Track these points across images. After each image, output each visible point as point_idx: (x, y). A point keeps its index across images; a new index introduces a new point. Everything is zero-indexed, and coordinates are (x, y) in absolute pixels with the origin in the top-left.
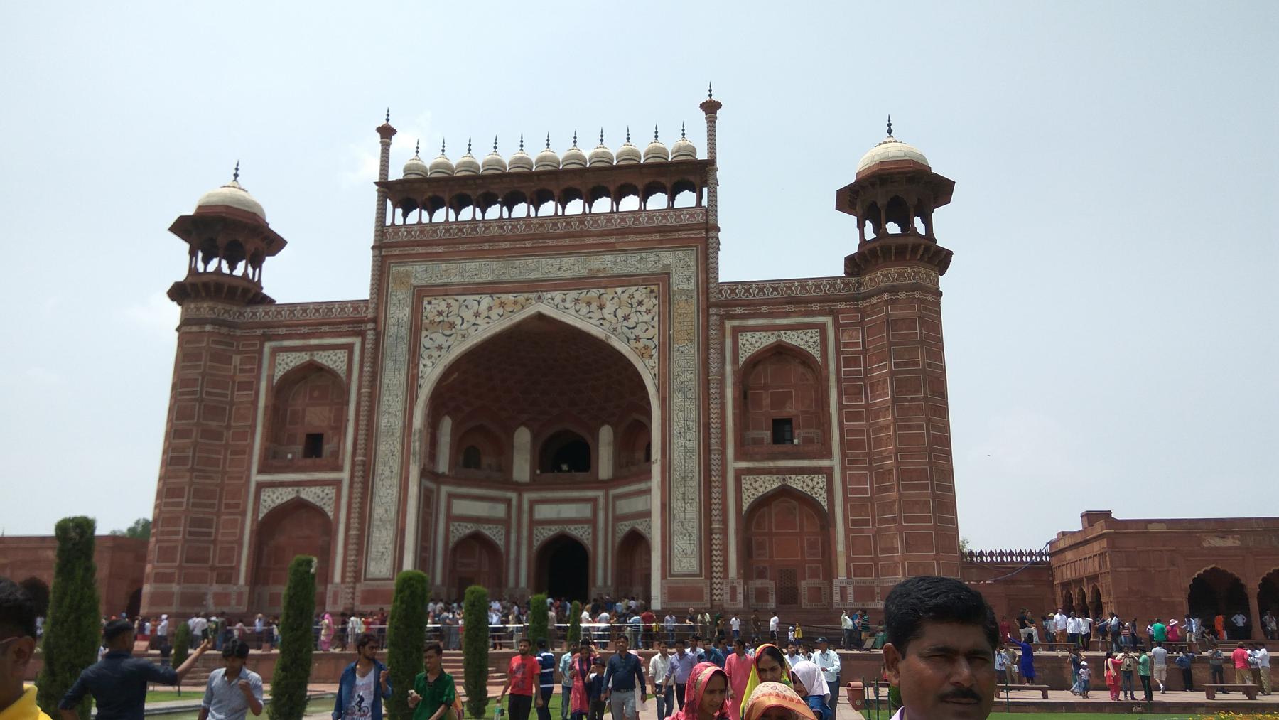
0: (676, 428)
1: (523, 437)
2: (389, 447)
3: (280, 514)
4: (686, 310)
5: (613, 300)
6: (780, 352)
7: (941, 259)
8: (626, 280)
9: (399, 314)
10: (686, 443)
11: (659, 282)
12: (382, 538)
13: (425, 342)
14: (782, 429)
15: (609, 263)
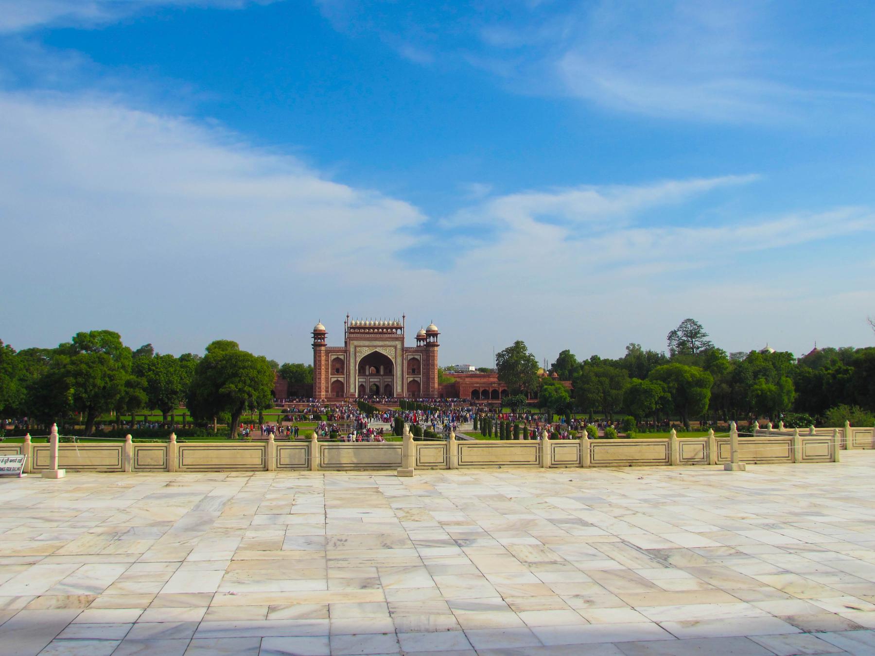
0: (398, 370)
1: (367, 367)
2: (352, 372)
3: (335, 382)
4: (399, 352)
5: (388, 349)
6: (414, 358)
7: (438, 346)
8: (390, 346)
9: (352, 350)
10: (399, 373)
11: (395, 347)
12: (352, 386)
13: (358, 354)
14: (414, 371)
15: (387, 343)
